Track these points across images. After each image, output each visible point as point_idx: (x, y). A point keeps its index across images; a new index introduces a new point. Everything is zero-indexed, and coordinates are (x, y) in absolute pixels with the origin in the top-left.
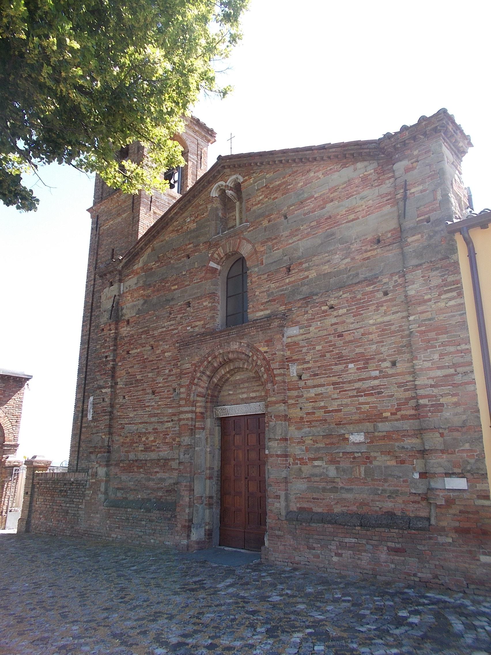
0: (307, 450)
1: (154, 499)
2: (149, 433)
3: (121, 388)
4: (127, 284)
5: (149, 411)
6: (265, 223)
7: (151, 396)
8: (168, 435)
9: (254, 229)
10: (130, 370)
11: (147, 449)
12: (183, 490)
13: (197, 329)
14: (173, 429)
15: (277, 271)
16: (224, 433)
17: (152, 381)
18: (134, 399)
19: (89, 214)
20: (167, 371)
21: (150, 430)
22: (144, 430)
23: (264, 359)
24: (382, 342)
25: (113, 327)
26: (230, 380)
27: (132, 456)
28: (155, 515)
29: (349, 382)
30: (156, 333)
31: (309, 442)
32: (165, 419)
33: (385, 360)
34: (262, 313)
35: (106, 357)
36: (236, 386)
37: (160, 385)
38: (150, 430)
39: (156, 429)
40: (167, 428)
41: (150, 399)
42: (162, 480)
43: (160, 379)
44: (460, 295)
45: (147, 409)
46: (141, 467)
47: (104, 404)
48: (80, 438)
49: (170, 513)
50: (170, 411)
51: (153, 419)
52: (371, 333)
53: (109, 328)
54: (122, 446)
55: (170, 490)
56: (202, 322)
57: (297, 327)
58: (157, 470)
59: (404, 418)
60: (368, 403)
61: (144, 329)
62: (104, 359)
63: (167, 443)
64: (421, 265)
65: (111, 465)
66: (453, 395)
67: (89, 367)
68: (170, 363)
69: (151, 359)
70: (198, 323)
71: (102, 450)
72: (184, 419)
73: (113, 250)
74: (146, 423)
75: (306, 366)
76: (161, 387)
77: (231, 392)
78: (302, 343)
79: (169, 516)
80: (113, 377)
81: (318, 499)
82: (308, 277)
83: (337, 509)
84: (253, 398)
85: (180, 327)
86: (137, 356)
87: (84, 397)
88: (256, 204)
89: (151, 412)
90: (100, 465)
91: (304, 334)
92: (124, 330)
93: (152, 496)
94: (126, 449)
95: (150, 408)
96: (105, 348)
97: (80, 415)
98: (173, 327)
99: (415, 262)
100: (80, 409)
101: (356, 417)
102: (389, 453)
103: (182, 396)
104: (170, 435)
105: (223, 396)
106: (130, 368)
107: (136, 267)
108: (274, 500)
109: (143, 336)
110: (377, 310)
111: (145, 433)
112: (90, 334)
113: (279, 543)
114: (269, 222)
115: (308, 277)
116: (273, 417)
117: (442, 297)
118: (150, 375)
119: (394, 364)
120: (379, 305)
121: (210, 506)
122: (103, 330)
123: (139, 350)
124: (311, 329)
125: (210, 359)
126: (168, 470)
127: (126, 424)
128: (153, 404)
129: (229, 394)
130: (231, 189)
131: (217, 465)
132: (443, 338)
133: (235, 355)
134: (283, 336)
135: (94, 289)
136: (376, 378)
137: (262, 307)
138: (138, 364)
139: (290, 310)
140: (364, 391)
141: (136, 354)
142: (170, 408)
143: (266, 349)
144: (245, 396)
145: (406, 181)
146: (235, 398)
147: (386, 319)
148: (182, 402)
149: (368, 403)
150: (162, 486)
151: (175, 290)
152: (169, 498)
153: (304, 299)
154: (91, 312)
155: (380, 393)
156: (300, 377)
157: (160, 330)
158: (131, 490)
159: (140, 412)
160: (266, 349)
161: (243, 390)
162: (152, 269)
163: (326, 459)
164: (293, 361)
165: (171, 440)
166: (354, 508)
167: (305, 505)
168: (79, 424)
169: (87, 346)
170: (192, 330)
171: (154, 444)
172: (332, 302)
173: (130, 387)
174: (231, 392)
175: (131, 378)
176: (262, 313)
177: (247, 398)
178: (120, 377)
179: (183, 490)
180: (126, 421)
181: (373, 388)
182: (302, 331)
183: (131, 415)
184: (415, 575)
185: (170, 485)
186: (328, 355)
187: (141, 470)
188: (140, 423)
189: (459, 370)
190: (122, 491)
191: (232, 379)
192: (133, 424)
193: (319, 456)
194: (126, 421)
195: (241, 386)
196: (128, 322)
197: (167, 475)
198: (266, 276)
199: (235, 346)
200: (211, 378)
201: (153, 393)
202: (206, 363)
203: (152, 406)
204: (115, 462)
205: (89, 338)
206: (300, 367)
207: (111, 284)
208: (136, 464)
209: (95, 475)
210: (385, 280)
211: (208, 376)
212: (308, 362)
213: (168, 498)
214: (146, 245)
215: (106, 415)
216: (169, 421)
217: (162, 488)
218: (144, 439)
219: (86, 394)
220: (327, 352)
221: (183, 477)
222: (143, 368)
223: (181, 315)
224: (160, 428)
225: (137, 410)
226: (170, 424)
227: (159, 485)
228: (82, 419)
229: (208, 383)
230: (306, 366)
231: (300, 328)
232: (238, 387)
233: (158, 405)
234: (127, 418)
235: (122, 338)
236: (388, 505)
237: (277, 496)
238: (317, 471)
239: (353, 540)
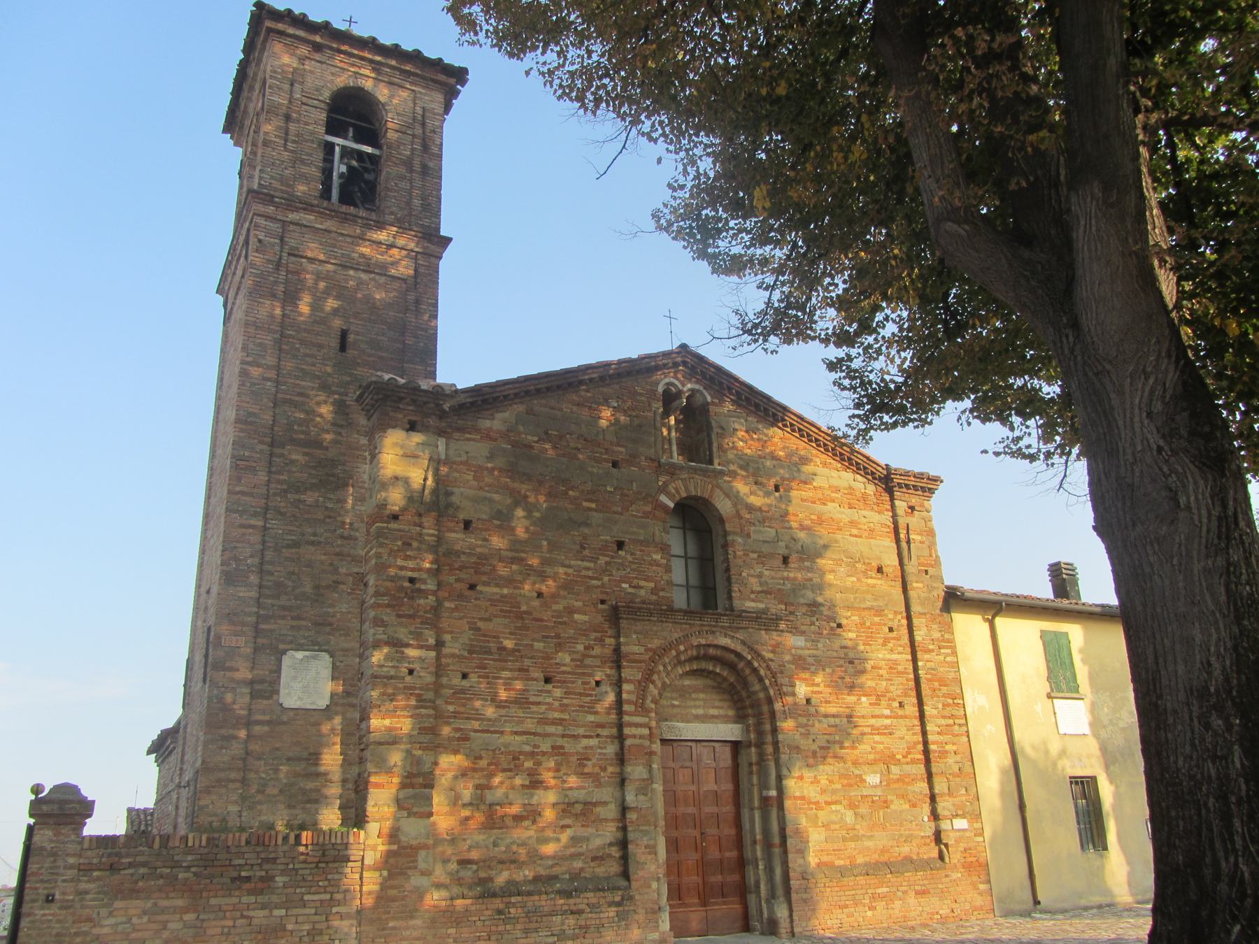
0: (823, 792)
2: (544, 754)
8: (590, 760)
10: (480, 624)
12: (643, 853)
13: (642, 592)
15: (771, 556)
17: (543, 658)
20: (580, 647)
22: (527, 748)
23: (769, 668)
24: (891, 680)
28: (586, 901)
29: (863, 717)
31: (824, 782)
32: (581, 731)
33: (894, 700)
34: (753, 604)
37: (563, 669)
38: (545, 746)
39: (562, 747)
40: (586, 748)
41: (541, 691)
43: (564, 657)
45: (534, 708)
49: (620, 893)
50: (591, 718)
51: (551, 729)
52: (880, 668)
56: (652, 585)
57: (803, 638)
60: (882, 743)
61: (517, 555)
62: (407, 584)
64: (925, 614)
66: (953, 744)
68: (586, 635)
72: (634, 736)
74: (534, 734)
75: (816, 689)
76: (564, 673)
77: (676, 703)
78: (811, 660)
81: (840, 850)
83: (860, 860)
84: (713, 717)
85: (606, 579)
86: (500, 601)
89: (545, 716)
93: (557, 870)
95: (544, 707)
98: (590, 573)
101: (871, 757)
104: (594, 761)
106: (480, 619)
107: (486, 424)
110: (884, 644)
111: (532, 754)
113: (806, 909)
115: (811, 580)
118: (539, 645)
120: (886, 641)
123: (505, 591)
125: (682, 648)
126: (594, 822)
127: (476, 731)
128: (550, 700)
129: (673, 706)
132: (944, 690)
133: (719, 653)
137: (753, 596)
138: (504, 617)
140: (878, 729)
141: (498, 597)
142: (591, 713)
144: (700, 711)
146: (683, 712)
147: (894, 657)
149: (882, 743)
150: (580, 850)
152: (602, 869)
153: (809, 605)
155: (890, 734)
161: (698, 703)
162: (532, 447)
163: (845, 802)
165: (597, 770)
166: (876, 856)
167: (825, 859)
174: (676, 703)
176: (753, 604)
178: (451, 632)
179: (643, 853)
180: (476, 725)
181: (886, 727)
182: (808, 644)
184: (937, 913)
185: (598, 849)
189: (957, 721)
190: (475, 867)
193: (837, 798)
194: (476, 725)
195: (693, 696)
196: (467, 524)
197: (591, 830)
198: (755, 556)
201: (547, 680)
202: (674, 652)
203: (549, 704)
210: (891, 616)
212: (818, 685)
213: (597, 870)
216: (591, 737)
217: (583, 854)
221: (642, 831)
222: (520, 628)
223: (607, 559)
224: (569, 746)
225: (509, 707)
226: (593, 742)
230: (816, 689)
236: (905, 850)
238: (833, 817)
239: (885, 890)
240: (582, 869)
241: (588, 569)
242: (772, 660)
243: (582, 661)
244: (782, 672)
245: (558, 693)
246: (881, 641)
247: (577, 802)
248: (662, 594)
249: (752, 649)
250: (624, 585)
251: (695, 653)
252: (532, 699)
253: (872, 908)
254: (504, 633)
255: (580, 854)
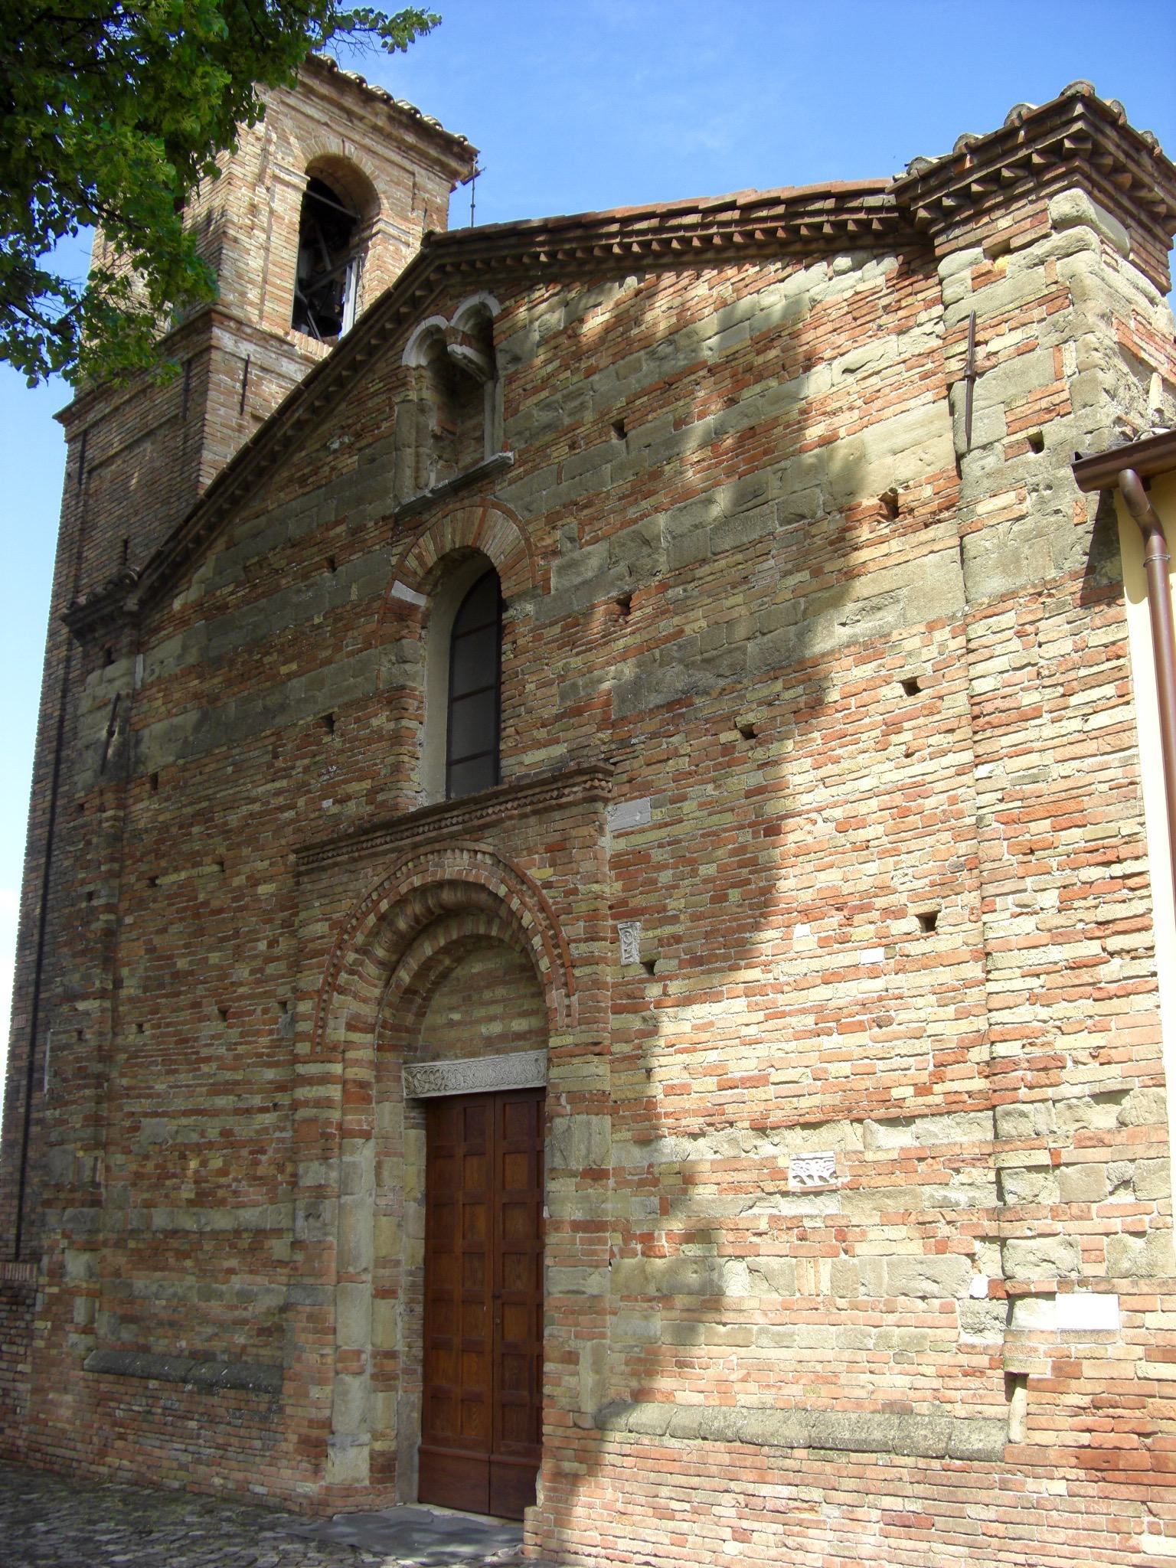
1: (223, 1352)
2: (210, 1145)
3: (131, 999)
4: (159, 653)
5: (210, 1076)
6: (560, 452)
7: (218, 1026)
9: (527, 473)
10: (157, 940)
11: (204, 1198)
12: (304, 1330)
13: (351, 807)
14: (278, 1134)
16: (436, 1155)
18: (168, 1034)
19: (60, 430)
20: (262, 946)
21: (213, 1134)
22: (194, 1137)
23: (543, 907)
25: (109, 797)
26: (454, 975)
27: (160, 1219)
30: (234, 819)
32: (257, 1101)
33: (899, 913)
35: (90, 896)
36: (470, 997)
37: (241, 990)
38: (213, 1134)
41: (213, 1037)
42: (245, 1297)
43: (243, 972)
44: (1124, 698)
46: (186, 1255)
47: (81, 1050)
48: (24, 1156)
50: (270, 1074)
51: (221, 1101)
53: (97, 802)
54: (134, 1185)
55: (268, 1329)
56: (367, 784)
58: (233, 1263)
59: (952, 1107)
61: (198, 807)
62: (84, 905)
63: (261, 1178)
64: (1012, 595)
65: (105, 1244)
67: (48, 929)
69: (215, 904)
70: (354, 787)
71: (78, 1195)
72: (306, 1103)
73: (126, 542)
75: (668, 930)
76: (242, 997)
78: (657, 856)
79: (263, 1407)
80: (109, 962)
82: (682, 631)
83: (748, 1396)
85: (301, 802)
86: (177, 895)
87: (34, 1026)
88: (536, 390)
90: (72, 1243)
91: (666, 825)
92: (145, 810)
93: (217, 1345)
94: (146, 1196)
95: (214, 1065)
96: (86, 867)
97: (24, 1082)
99: (995, 584)
100: (24, 1063)
102: (904, 1217)
103: (304, 1026)
104: (270, 1153)
105: (433, 1029)
108: (560, 1366)
109: (195, 830)
112: (52, 821)
114: (573, 446)
116: (563, 1101)
117: (1073, 700)
118: (214, 958)
119: (929, 922)
120: (893, 727)
121: (383, 1379)
122: (81, 807)
123: (183, 875)
124: (688, 806)
127: (146, 1115)
128: (222, 1050)
129: (451, 1024)
130: (466, 340)
131: (410, 1248)
134: (601, 830)
135: (67, 673)
136: (874, 972)
138: (181, 920)
139: (624, 743)
142: (270, 1065)
143: (547, 873)
144: (496, 1028)
145: (974, 317)
146: (466, 1035)
148: (303, 1048)
151: (290, 676)
152: (265, 1352)
153: (670, 706)
154: (58, 751)
156: (649, 966)
157: (245, 809)
158: (161, 1324)
159: (184, 1078)
160: (547, 873)
164: (633, 914)
165: (272, 1171)
166: (795, 1390)
168: (22, 1110)
169: (43, 860)
170: (335, 810)
171: (223, 1180)
172: (750, 718)
173: (158, 997)
175: (161, 967)
176: (541, 755)
177: (503, 1037)
178: (128, 964)
179: (304, 1330)
180: (146, 1104)
183: (160, 1087)
185: (269, 1312)
186: (734, 895)
187: (188, 1263)
188: (186, 1113)
189: (1114, 943)
191: (459, 972)
192: (164, 1114)
194: (146, 1104)
195: (487, 995)
196: (154, 780)
198: (557, 629)
199: (456, 864)
200: (390, 968)
203: (220, 1058)
204: (113, 1236)
205: (51, 833)
206: (650, 934)
207: (110, 661)
208: (174, 1243)
209: (58, 1272)
210: (909, 645)
211: (381, 963)
212: (674, 920)
214: (210, 528)
215: (86, 1086)
218: (193, 1164)
219: (41, 1015)
220: (733, 886)
223: (306, 761)
224: (244, 1129)
226: (269, 1118)
227: (236, 1313)
228: (29, 1097)
229: (381, 983)
230: (668, 930)
231: (654, 807)
232: (475, 997)
233: (237, 1058)
234: (149, 1096)
235: (137, 835)
236: (894, 1383)
237: (570, 1353)
240: (244, 1347)
241: (278, 793)
242: (548, 885)
243: (261, 970)
244: (568, 911)
245: (234, 1034)
246: (868, 739)
247: (246, 1230)
248: (380, 797)
249: (509, 868)
250: (327, 804)
251: (417, 908)
252: (205, 1052)
253: (742, 1536)
254: (178, 947)
255: (244, 1322)
